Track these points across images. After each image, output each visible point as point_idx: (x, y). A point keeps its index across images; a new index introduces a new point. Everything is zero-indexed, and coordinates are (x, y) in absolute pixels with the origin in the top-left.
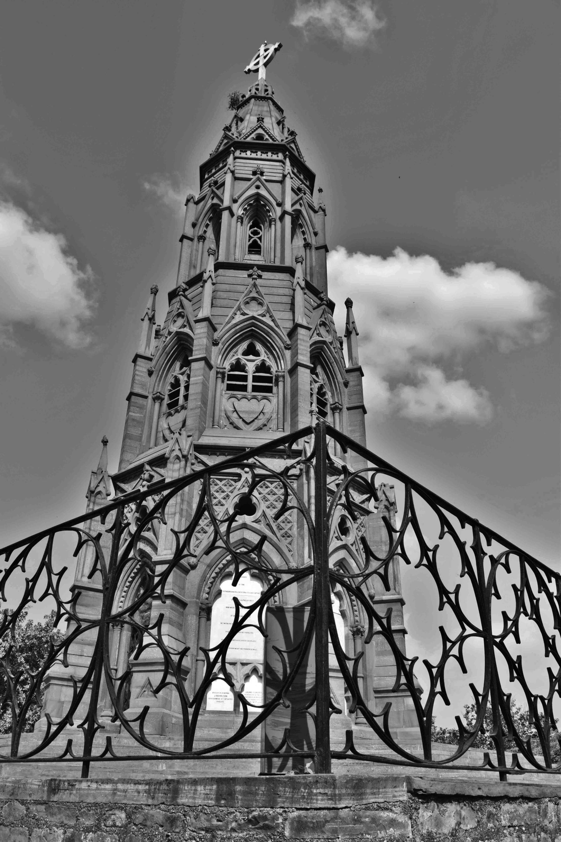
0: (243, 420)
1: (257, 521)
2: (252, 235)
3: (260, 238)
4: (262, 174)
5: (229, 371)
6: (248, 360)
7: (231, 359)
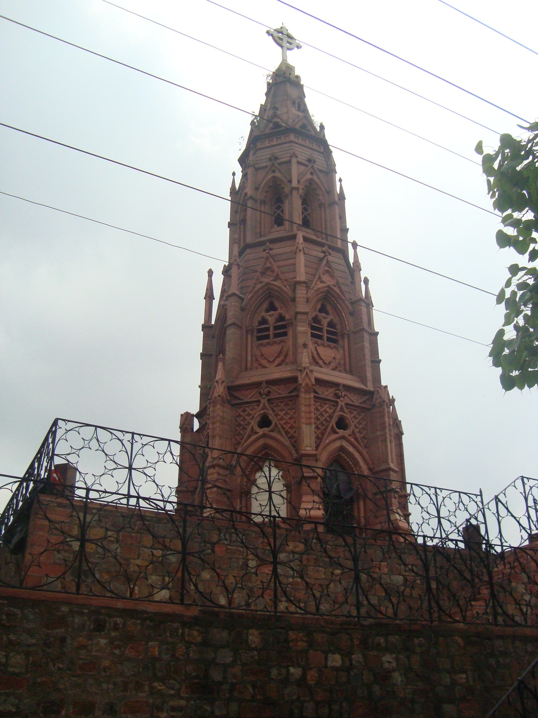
0: (269, 361)
1: (272, 431)
2: (276, 210)
3: (282, 211)
4: (276, 158)
5: (258, 326)
6: (270, 316)
7: (257, 318)
